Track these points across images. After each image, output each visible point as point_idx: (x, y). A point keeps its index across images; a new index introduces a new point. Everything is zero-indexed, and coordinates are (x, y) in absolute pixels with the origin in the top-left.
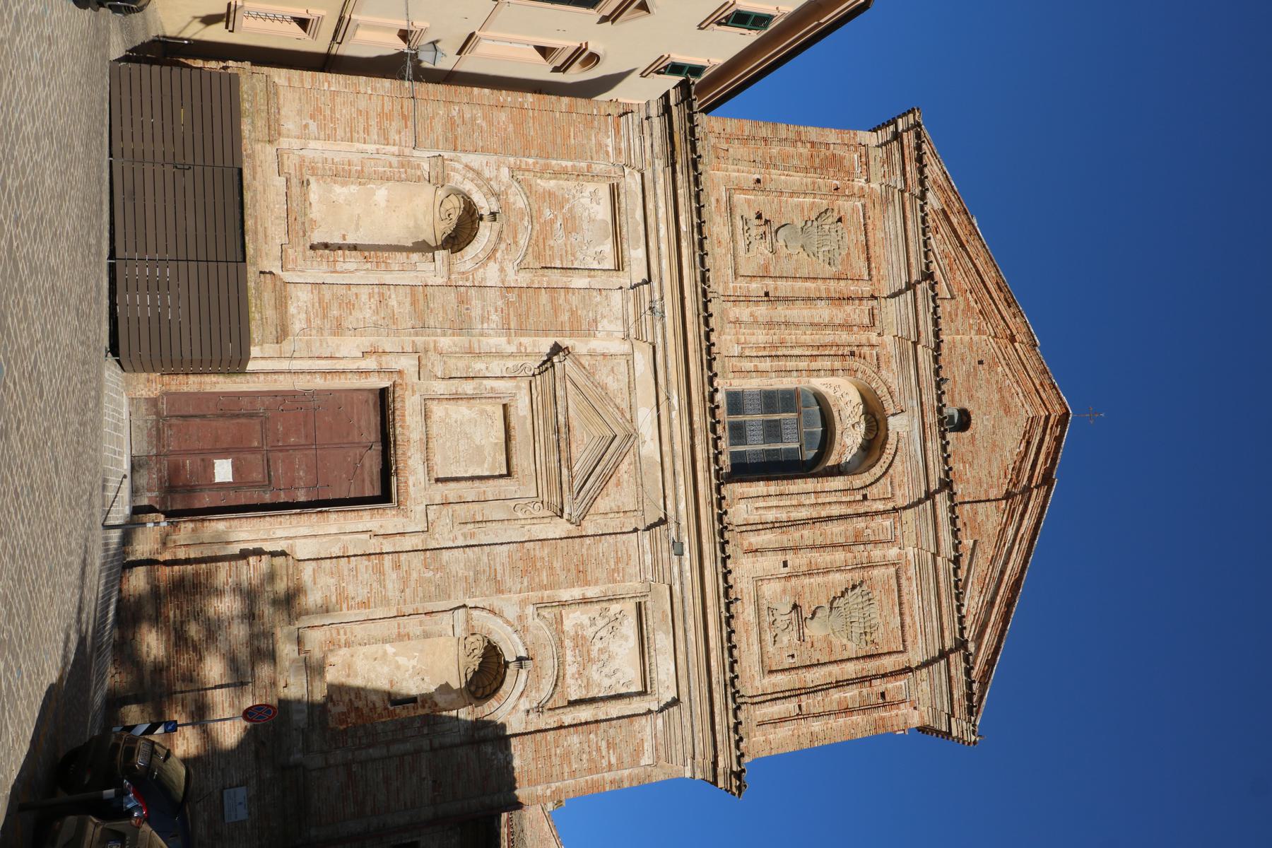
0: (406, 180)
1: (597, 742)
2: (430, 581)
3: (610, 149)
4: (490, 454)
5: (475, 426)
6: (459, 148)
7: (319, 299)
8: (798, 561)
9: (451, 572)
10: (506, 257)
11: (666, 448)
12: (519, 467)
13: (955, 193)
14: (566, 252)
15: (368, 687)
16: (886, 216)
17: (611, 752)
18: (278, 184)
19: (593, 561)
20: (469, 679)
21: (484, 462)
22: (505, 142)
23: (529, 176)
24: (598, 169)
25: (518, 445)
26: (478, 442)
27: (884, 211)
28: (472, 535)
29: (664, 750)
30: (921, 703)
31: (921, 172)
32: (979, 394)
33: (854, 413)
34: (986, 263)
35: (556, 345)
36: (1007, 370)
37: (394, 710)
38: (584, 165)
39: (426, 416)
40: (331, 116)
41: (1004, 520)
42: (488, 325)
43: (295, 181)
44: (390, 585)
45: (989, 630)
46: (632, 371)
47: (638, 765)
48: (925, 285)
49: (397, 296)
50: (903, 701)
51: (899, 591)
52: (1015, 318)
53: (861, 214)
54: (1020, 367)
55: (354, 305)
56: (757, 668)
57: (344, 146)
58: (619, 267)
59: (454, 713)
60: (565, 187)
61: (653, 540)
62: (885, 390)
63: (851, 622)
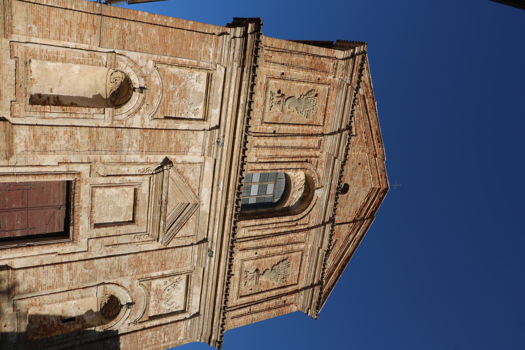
0: (92, 65)
1: (160, 333)
2: (87, 274)
3: (211, 54)
4: (124, 211)
5: (118, 198)
6: (126, 48)
7: (34, 134)
9: (98, 269)
10: (146, 112)
11: (213, 208)
12: (139, 218)
13: (372, 89)
14: (179, 108)
15: (50, 314)
16: (338, 94)
17: (166, 336)
18: (10, 63)
19: (170, 259)
20: (102, 307)
21: (121, 215)
22: (153, 46)
23: (163, 66)
24: (203, 64)
25: (140, 208)
26: (119, 206)
27: (338, 92)
28: (111, 251)
29: (189, 333)
30: (299, 303)
31: (360, 77)
32: (355, 178)
33: (300, 184)
34: (375, 122)
35: (166, 158)
36: (369, 168)
37: (63, 325)
38: (195, 62)
39: (92, 196)
40: (47, 23)
41: (350, 231)
42: (132, 149)
43: (21, 63)
44: (65, 278)
45: (332, 276)
46: (202, 171)
47: (177, 340)
48: (347, 132)
49: (81, 133)
50: (292, 303)
51: (301, 261)
52: (379, 147)
53: (327, 93)
54: (375, 167)
55: (55, 138)
59: (93, 328)
60: (183, 73)
61: (200, 249)
62: (317, 177)
63: (279, 274)
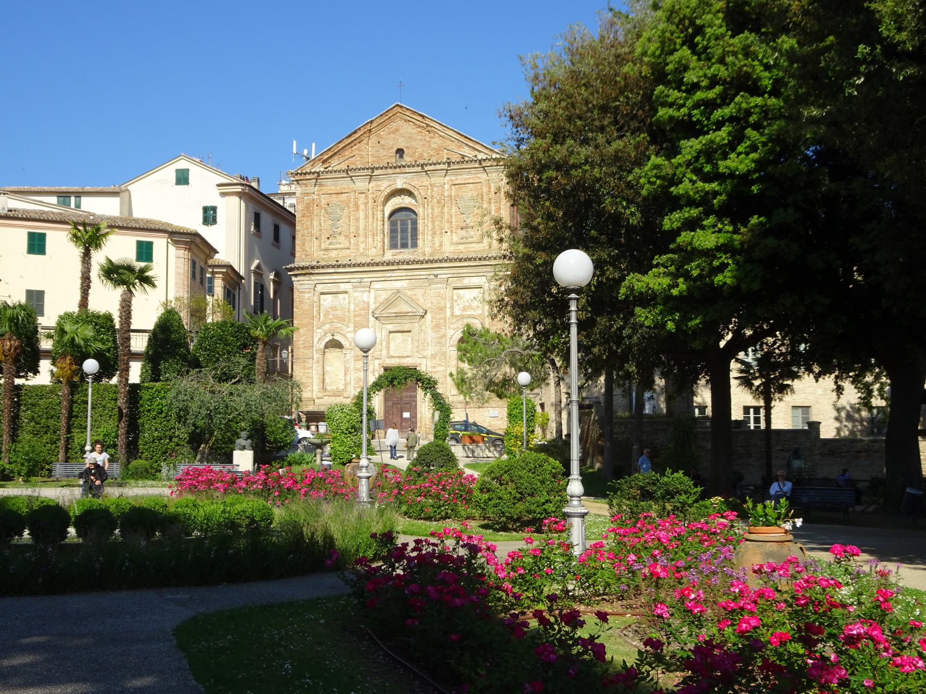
8: (446, 226)
11: (404, 278)
32: (391, 144)
56: (480, 245)
57: (314, 380)
58: (346, 292)
61: (433, 284)
